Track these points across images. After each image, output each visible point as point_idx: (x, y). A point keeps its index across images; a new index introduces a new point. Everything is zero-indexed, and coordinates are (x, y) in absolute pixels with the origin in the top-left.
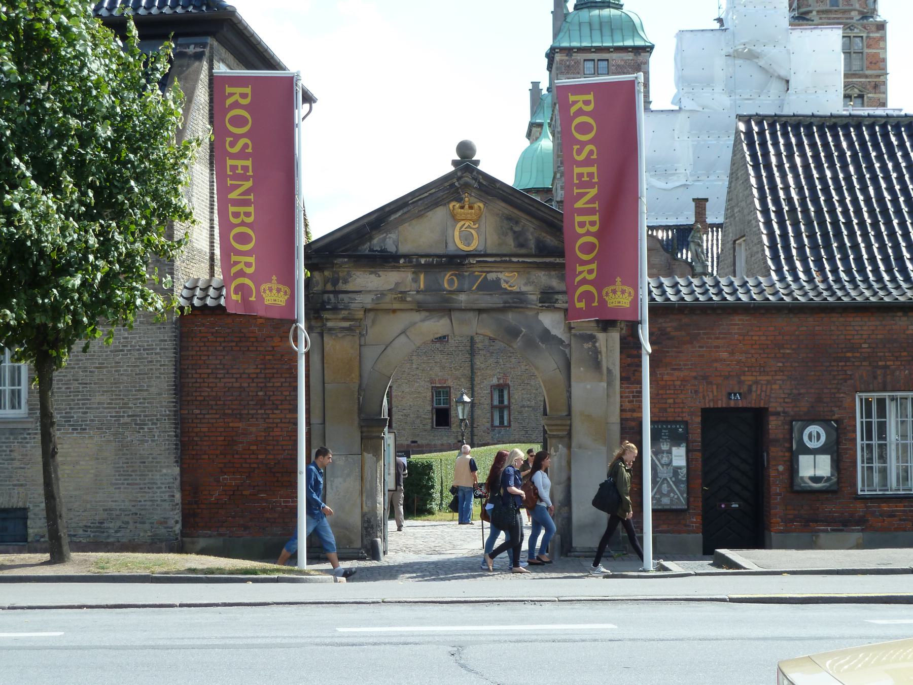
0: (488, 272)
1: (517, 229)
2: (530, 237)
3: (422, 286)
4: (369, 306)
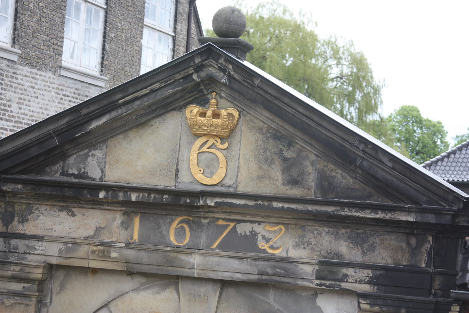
1: (288, 154)
2: (310, 169)
3: (136, 237)
4: (54, 261)
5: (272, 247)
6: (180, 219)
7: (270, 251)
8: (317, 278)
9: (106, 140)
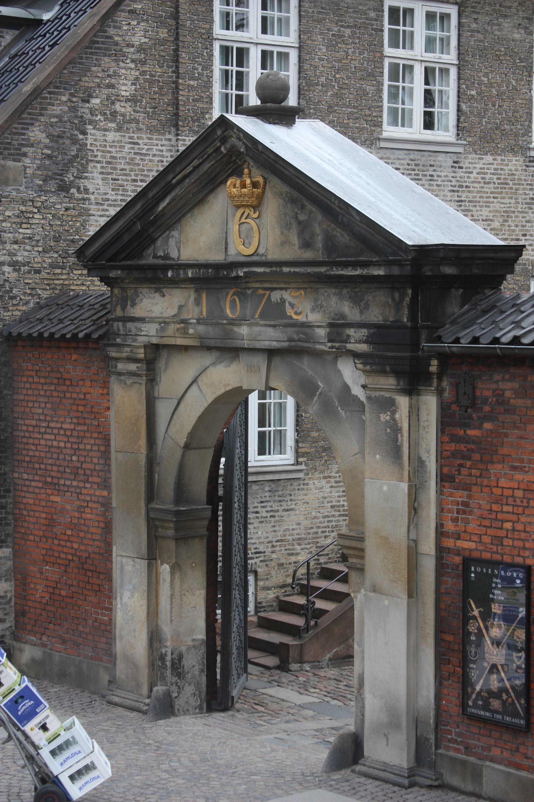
0: (272, 289)
2: (318, 231)
3: (204, 313)
4: (154, 341)
5: (296, 313)
6: (232, 291)
7: (295, 317)
8: (330, 341)
9: (179, 220)
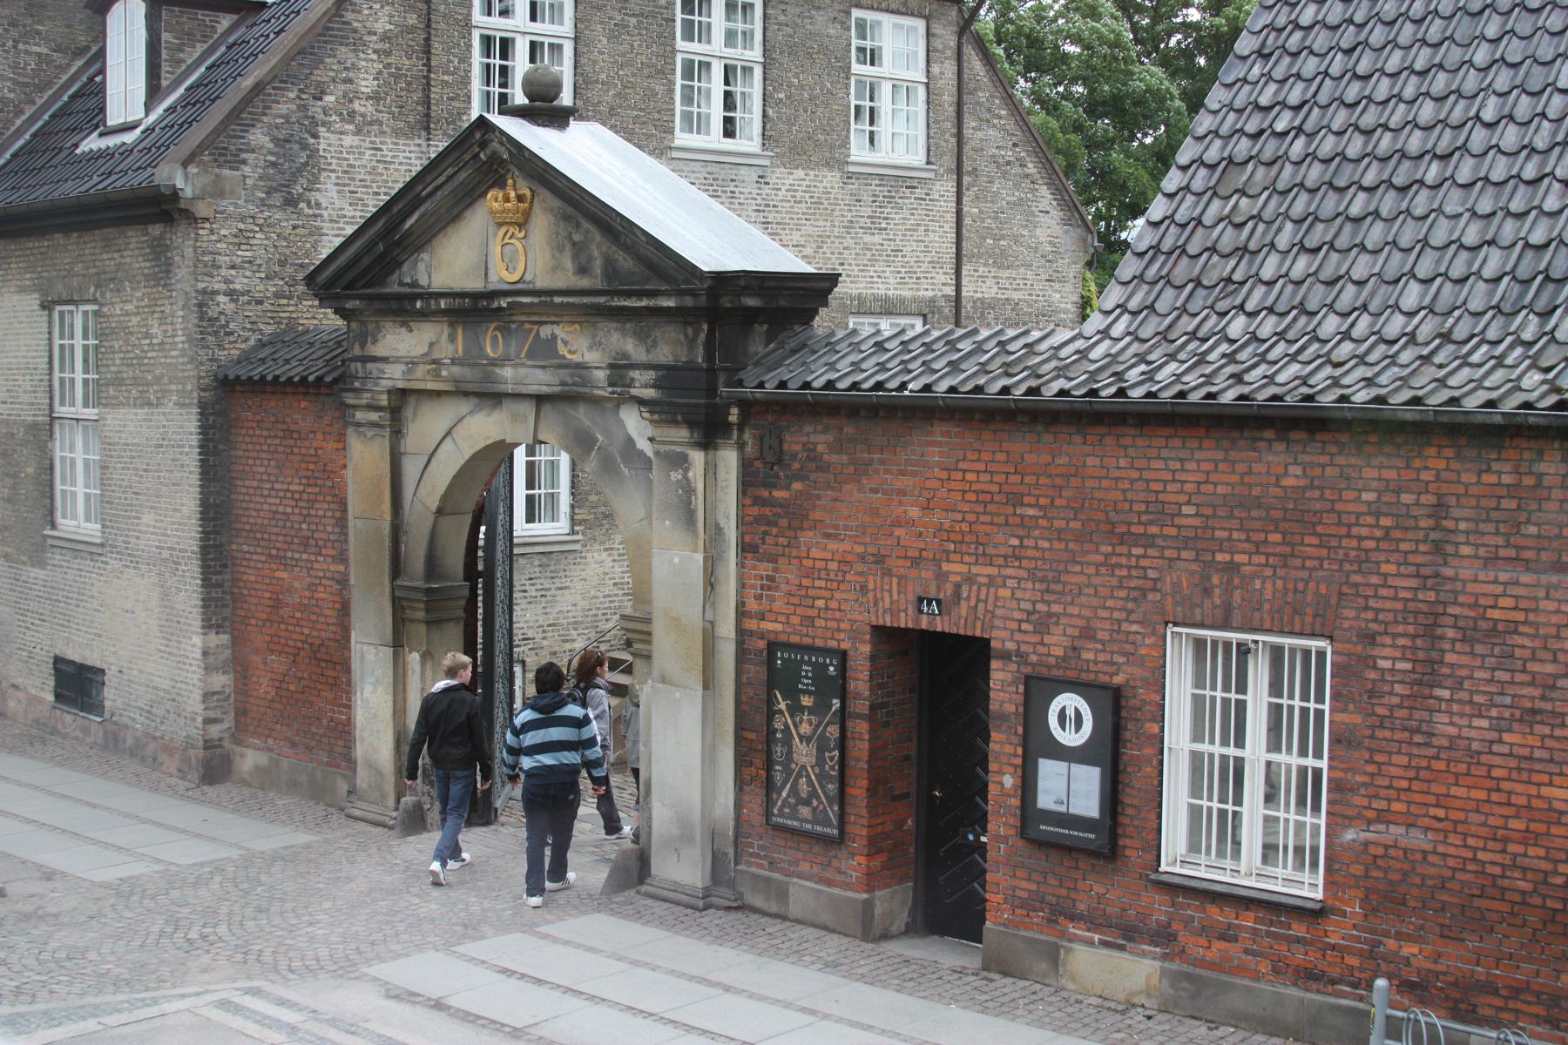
0: (542, 323)
1: (577, 237)
2: (596, 253)
4: (400, 385)
5: (570, 352)
6: (493, 326)
9: (430, 240)
